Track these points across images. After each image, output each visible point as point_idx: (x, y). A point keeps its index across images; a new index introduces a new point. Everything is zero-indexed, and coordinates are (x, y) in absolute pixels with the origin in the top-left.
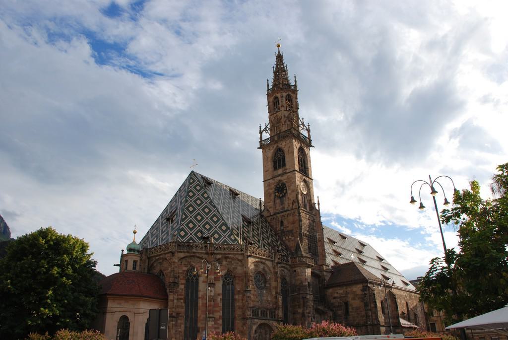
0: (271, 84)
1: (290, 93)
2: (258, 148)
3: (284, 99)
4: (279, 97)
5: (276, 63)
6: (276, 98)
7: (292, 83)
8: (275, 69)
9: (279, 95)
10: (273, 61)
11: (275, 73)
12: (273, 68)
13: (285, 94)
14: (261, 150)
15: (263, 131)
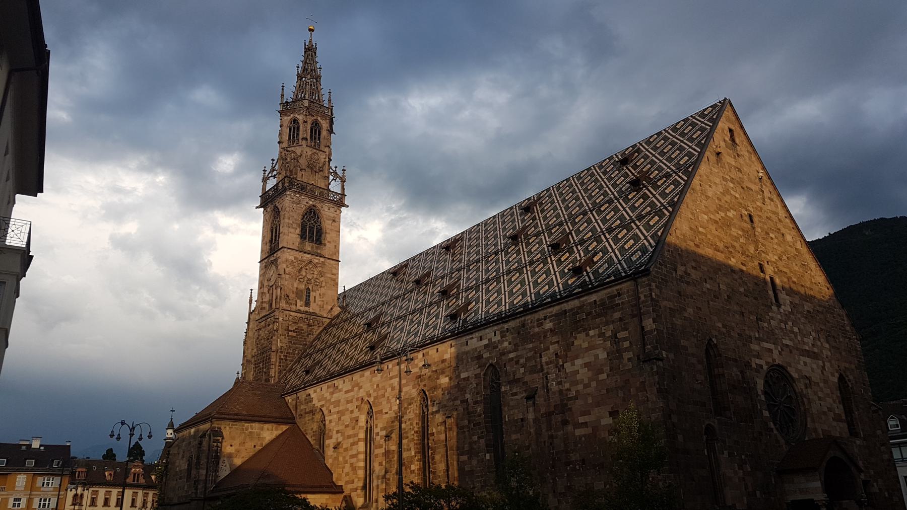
0: (289, 96)
1: (319, 118)
2: (257, 208)
3: (309, 127)
4: (301, 122)
5: (303, 59)
6: (295, 121)
7: (325, 98)
8: (300, 69)
9: (301, 118)
10: (298, 58)
11: (300, 77)
12: (298, 67)
13: (310, 120)
14: (262, 209)
15: (268, 178)
